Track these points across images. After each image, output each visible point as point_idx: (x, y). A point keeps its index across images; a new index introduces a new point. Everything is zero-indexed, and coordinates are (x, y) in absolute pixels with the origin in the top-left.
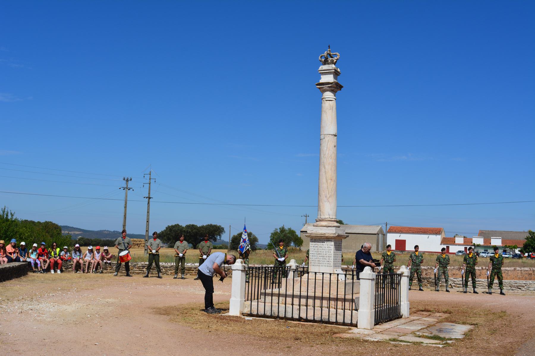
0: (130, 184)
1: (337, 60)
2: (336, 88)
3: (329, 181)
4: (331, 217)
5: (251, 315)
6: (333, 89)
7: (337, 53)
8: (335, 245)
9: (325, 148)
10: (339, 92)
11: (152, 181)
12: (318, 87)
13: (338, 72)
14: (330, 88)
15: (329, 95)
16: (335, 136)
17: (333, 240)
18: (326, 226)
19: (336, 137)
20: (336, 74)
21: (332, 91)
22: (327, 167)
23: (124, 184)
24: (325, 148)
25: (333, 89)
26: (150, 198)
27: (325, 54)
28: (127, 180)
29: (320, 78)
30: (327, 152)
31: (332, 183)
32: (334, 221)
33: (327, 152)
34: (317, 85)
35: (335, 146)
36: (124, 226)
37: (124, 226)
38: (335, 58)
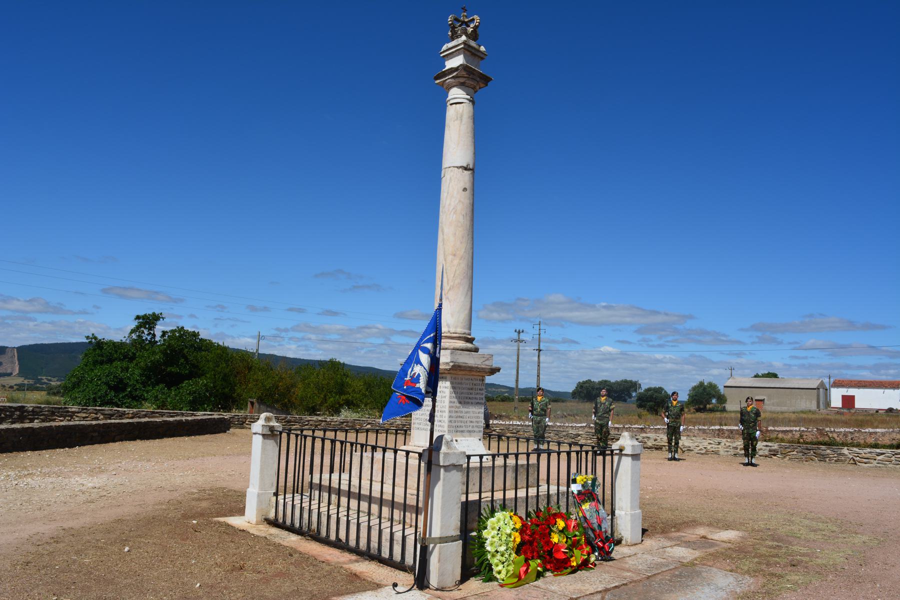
0: (522, 336)
1: (476, 27)
2: (473, 79)
3: (450, 258)
4: (452, 330)
5: (274, 523)
6: (462, 80)
7: (476, 17)
8: (453, 388)
9: (445, 194)
10: (484, 92)
11: (542, 332)
12: (438, 81)
13: (479, 51)
14: (457, 80)
15: (456, 93)
16: (466, 169)
17: (448, 376)
18: (462, 350)
19: (469, 172)
20: (468, 50)
21: (462, 85)
22: (446, 230)
23: (515, 336)
24: (445, 194)
25: (462, 80)
26: (540, 350)
27: (450, 19)
28: (519, 332)
29: (445, 67)
30: (448, 202)
31: (456, 262)
32: (459, 338)
33: (448, 202)
34: (437, 78)
35: (465, 189)
36: (517, 381)
37: (517, 381)
38: (472, 25)
